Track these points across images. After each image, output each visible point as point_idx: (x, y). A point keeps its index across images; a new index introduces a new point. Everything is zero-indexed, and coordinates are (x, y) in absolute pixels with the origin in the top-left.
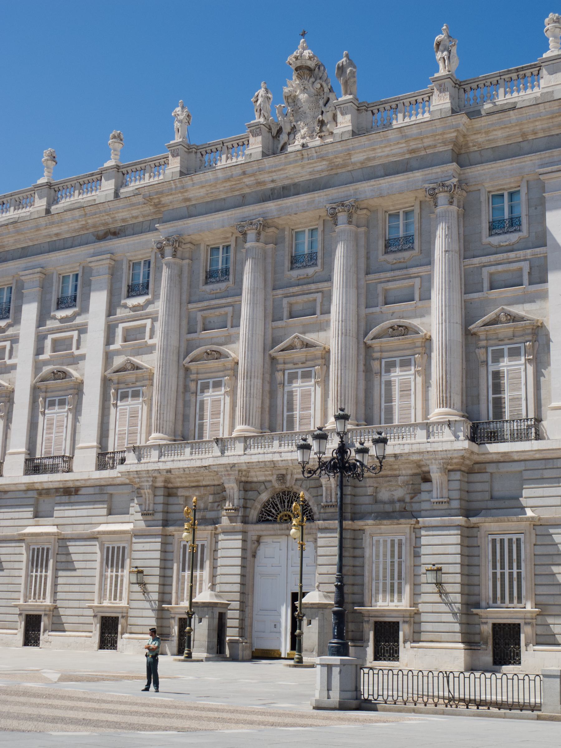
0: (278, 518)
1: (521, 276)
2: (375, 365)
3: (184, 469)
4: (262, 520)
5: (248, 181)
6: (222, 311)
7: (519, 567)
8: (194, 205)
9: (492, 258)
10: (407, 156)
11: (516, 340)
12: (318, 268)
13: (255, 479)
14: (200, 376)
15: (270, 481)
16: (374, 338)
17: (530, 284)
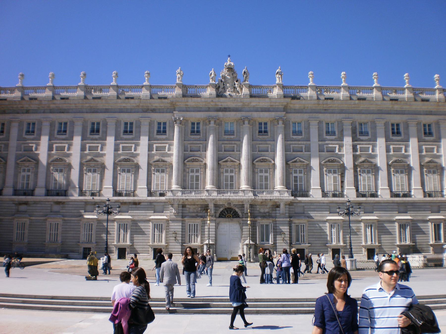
0: (226, 216)
1: (302, 149)
2: (256, 170)
3: (193, 199)
4: (220, 217)
5: (212, 103)
6: (198, 145)
7: (304, 233)
8: (189, 107)
9: (294, 142)
10: (269, 107)
11: (301, 168)
12: (235, 136)
13: (219, 204)
14: (190, 167)
15: (224, 205)
16: (256, 162)
17: (305, 152)
